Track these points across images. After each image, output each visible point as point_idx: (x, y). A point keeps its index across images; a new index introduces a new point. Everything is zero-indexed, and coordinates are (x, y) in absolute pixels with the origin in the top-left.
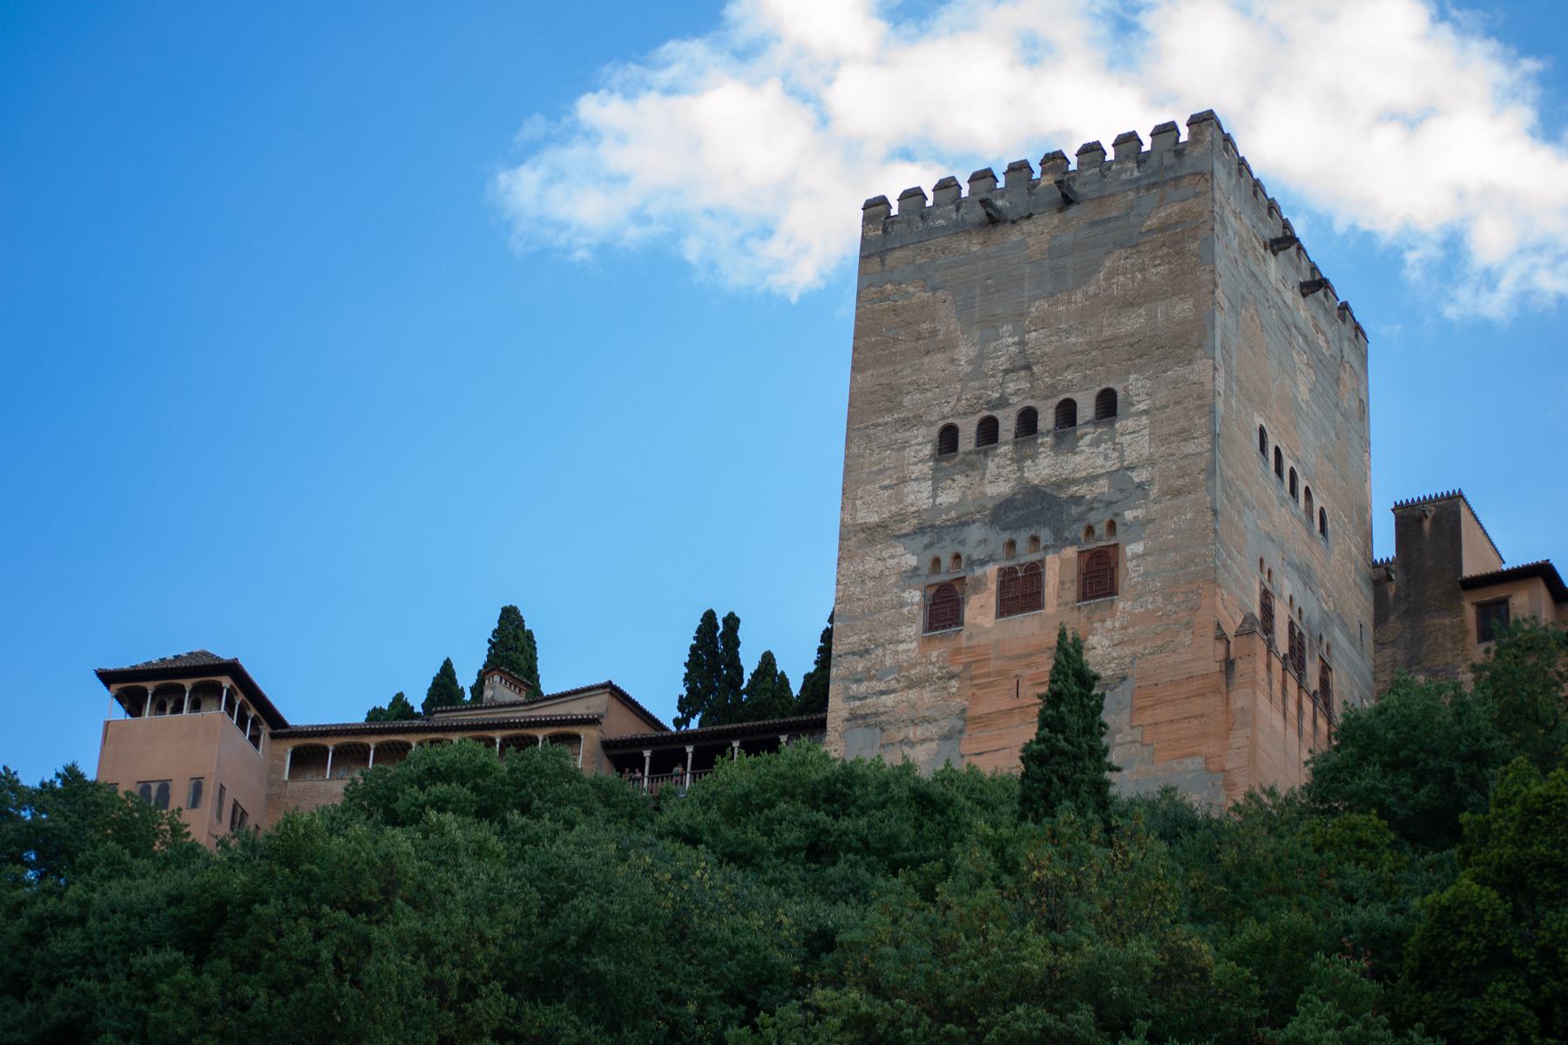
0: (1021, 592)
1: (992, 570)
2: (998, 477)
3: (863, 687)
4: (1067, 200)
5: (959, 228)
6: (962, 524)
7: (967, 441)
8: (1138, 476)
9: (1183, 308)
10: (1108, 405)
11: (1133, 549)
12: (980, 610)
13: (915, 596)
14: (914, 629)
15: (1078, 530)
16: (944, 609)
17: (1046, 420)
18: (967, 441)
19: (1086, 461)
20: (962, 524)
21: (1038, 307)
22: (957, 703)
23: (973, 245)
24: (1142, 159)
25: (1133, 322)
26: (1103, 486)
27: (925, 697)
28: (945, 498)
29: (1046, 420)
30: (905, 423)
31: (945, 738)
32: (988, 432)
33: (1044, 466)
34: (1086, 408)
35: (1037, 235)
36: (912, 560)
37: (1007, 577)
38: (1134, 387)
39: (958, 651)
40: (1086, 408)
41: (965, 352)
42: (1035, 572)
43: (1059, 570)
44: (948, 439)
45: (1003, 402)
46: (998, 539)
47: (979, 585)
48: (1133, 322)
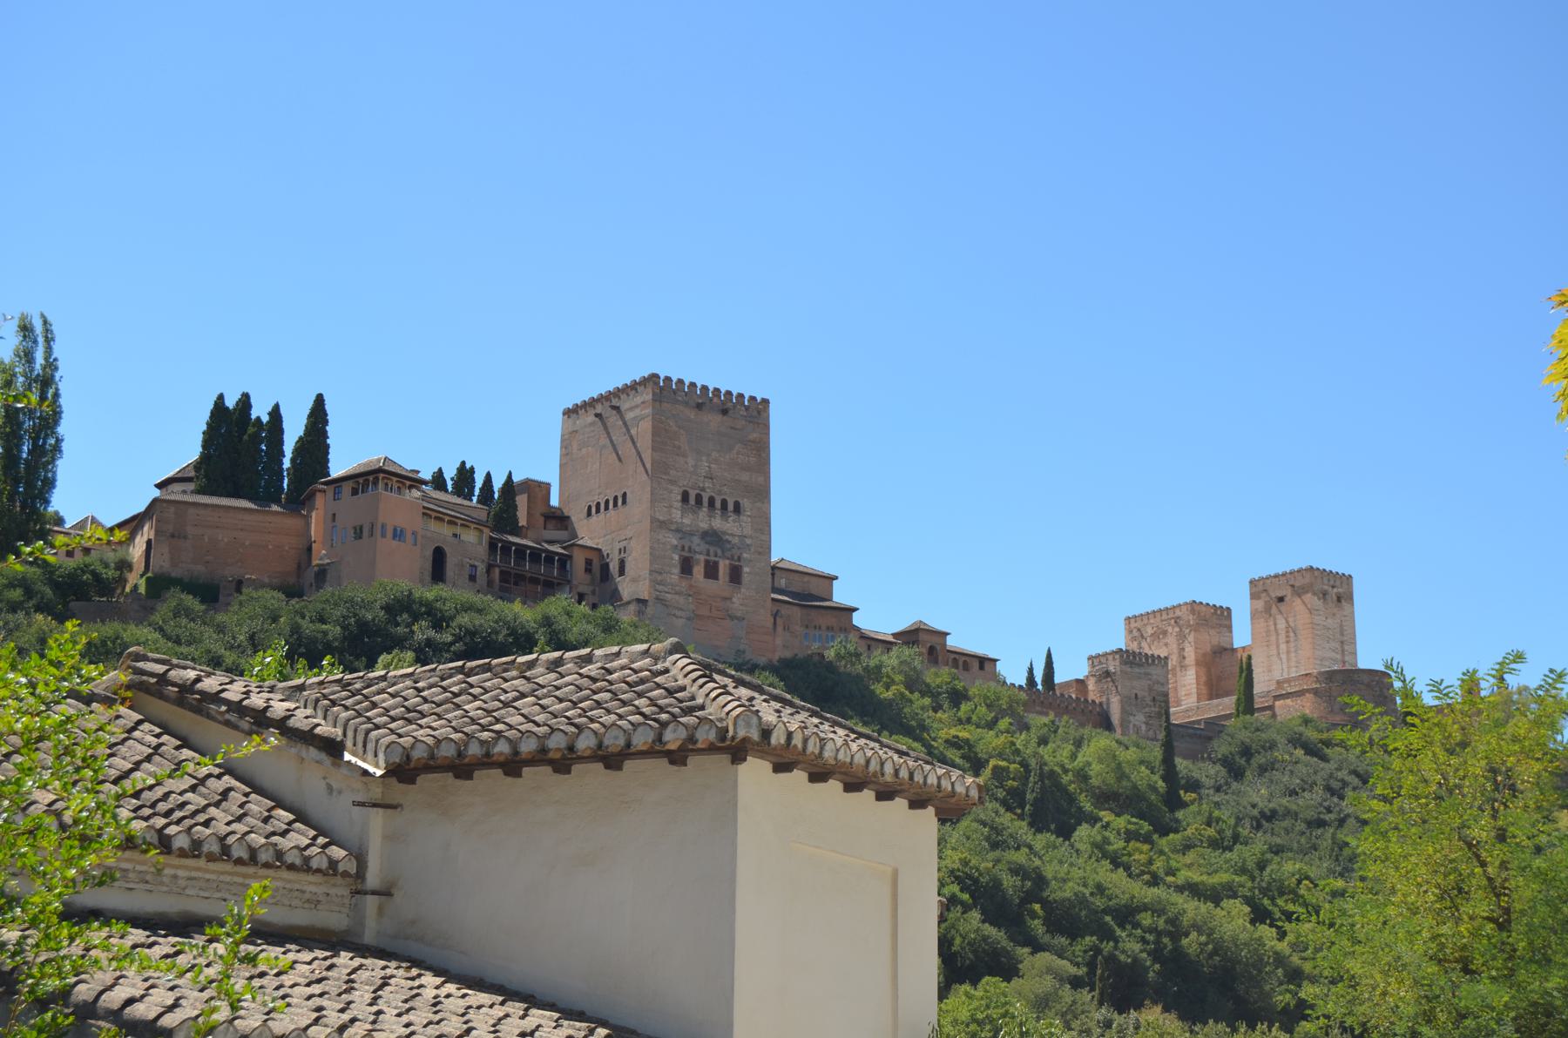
0: (711, 571)
1: (702, 558)
2: (703, 520)
3: (660, 588)
4: (725, 412)
5: (686, 404)
6: (692, 534)
7: (692, 501)
8: (748, 541)
9: (761, 479)
10: (737, 509)
11: (746, 569)
12: (698, 571)
13: (676, 557)
14: (676, 570)
15: (728, 554)
16: (686, 567)
17: (718, 504)
18: (692, 501)
19: (726, 525)
20: (692, 534)
21: (714, 454)
22: (692, 607)
23: (692, 414)
24: (747, 408)
25: (745, 477)
26: (736, 540)
27: (681, 600)
28: (686, 521)
29: (718, 504)
30: (673, 482)
31: (688, 619)
32: (699, 499)
33: (718, 523)
34: (731, 507)
35: (713, 420)
36: (675, 542)
37: (707, 562)
38: (746, 503)
39: (691, 586)
40: (731, 507)
41: (691, 462)
42: (716, 564)
43: (723, 567)
44: (685, 497)
45: (703, 489)
46: (704, 547)
47: (698, 562)
48: (745, 477)
